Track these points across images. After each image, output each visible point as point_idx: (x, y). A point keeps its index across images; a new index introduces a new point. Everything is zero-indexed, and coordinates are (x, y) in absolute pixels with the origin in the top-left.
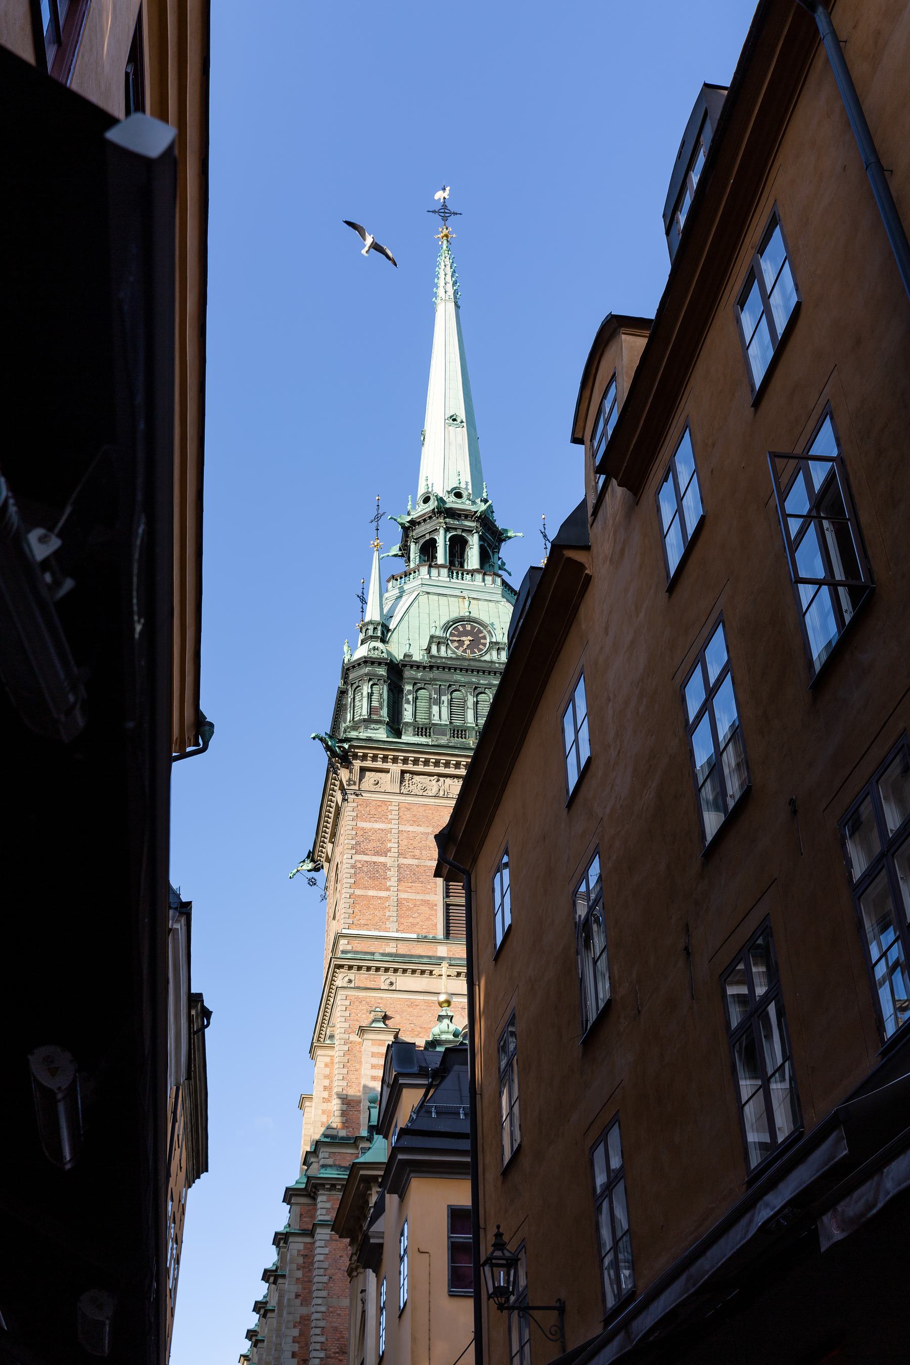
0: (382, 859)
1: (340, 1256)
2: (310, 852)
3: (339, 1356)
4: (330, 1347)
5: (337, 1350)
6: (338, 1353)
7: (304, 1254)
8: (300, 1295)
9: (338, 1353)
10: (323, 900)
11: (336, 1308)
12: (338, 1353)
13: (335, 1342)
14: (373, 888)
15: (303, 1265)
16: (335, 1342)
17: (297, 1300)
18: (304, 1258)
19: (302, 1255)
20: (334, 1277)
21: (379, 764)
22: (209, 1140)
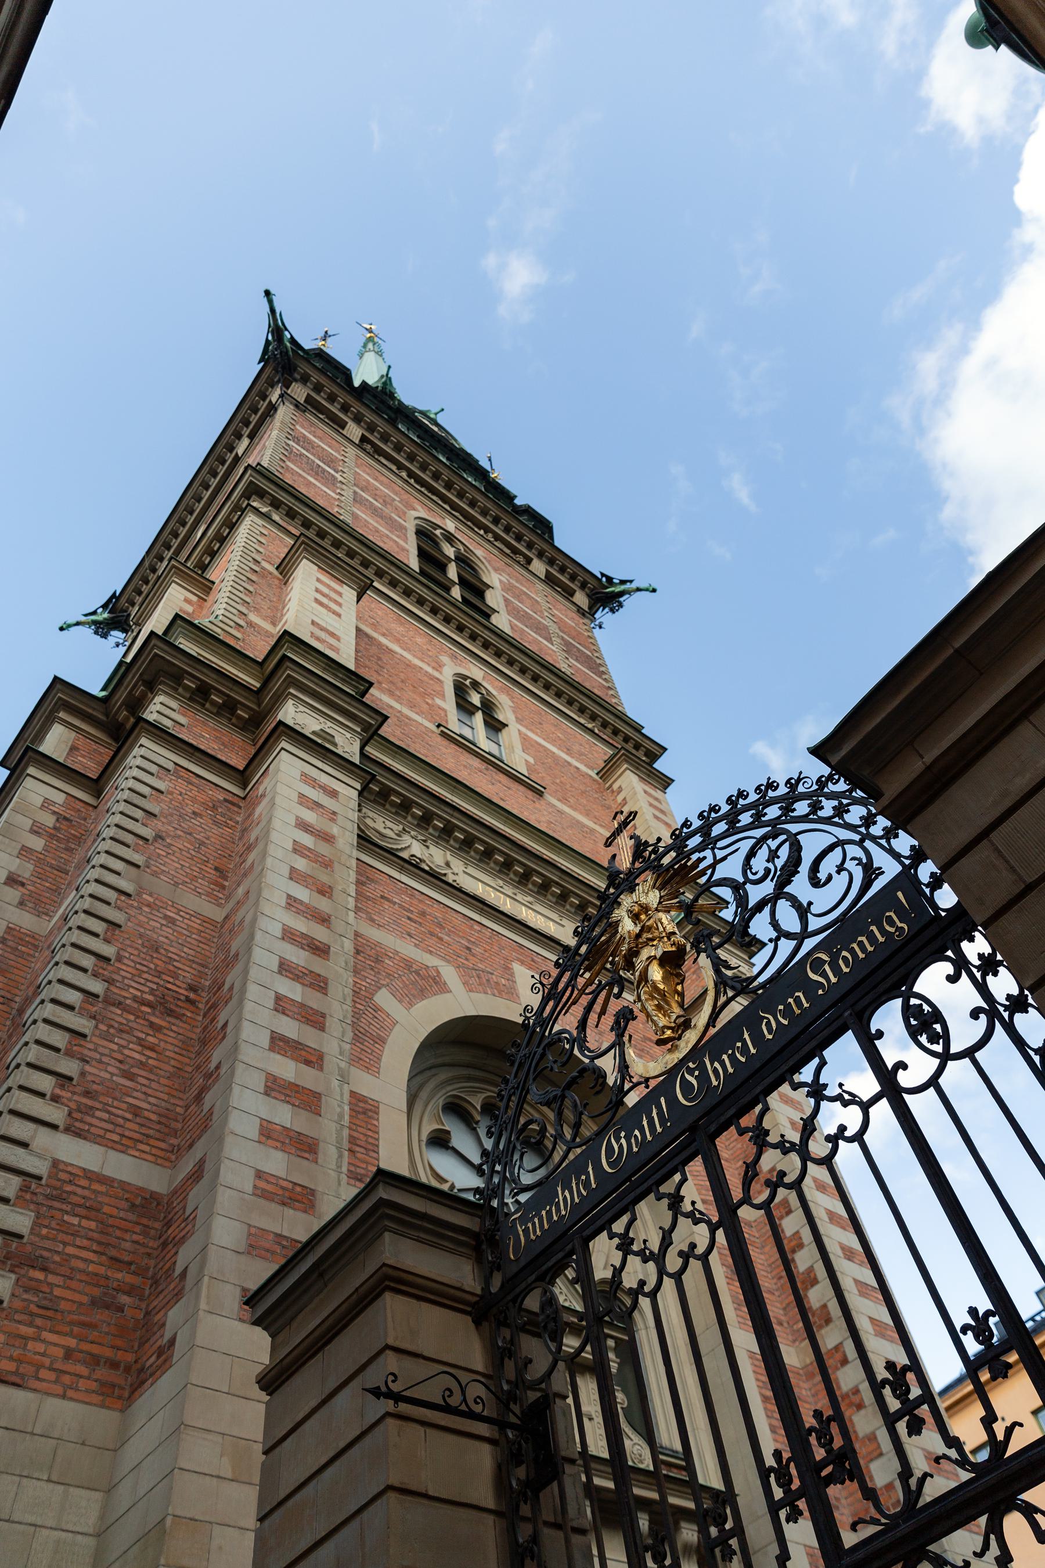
0: (332, 472)
1: (194, 813)
2: (115, 593)
3: (154, 1014)
4: (126, 981)
5: (151, 998)
6: (149, 1004)
7: (61, 812)
8: (23, 884)
9: (149, 1004)
10: (118, 646)
11: (166, 903)
12: (144, 1003)
13: (146, 976)
14: (316, 479)
15: (52, 831)
16: (146, 976)
17: (7, 888)
18: (57, 820)
19: (54, 813)
20: (168, 841)
21: (334, 409)
22: (10, 111)
